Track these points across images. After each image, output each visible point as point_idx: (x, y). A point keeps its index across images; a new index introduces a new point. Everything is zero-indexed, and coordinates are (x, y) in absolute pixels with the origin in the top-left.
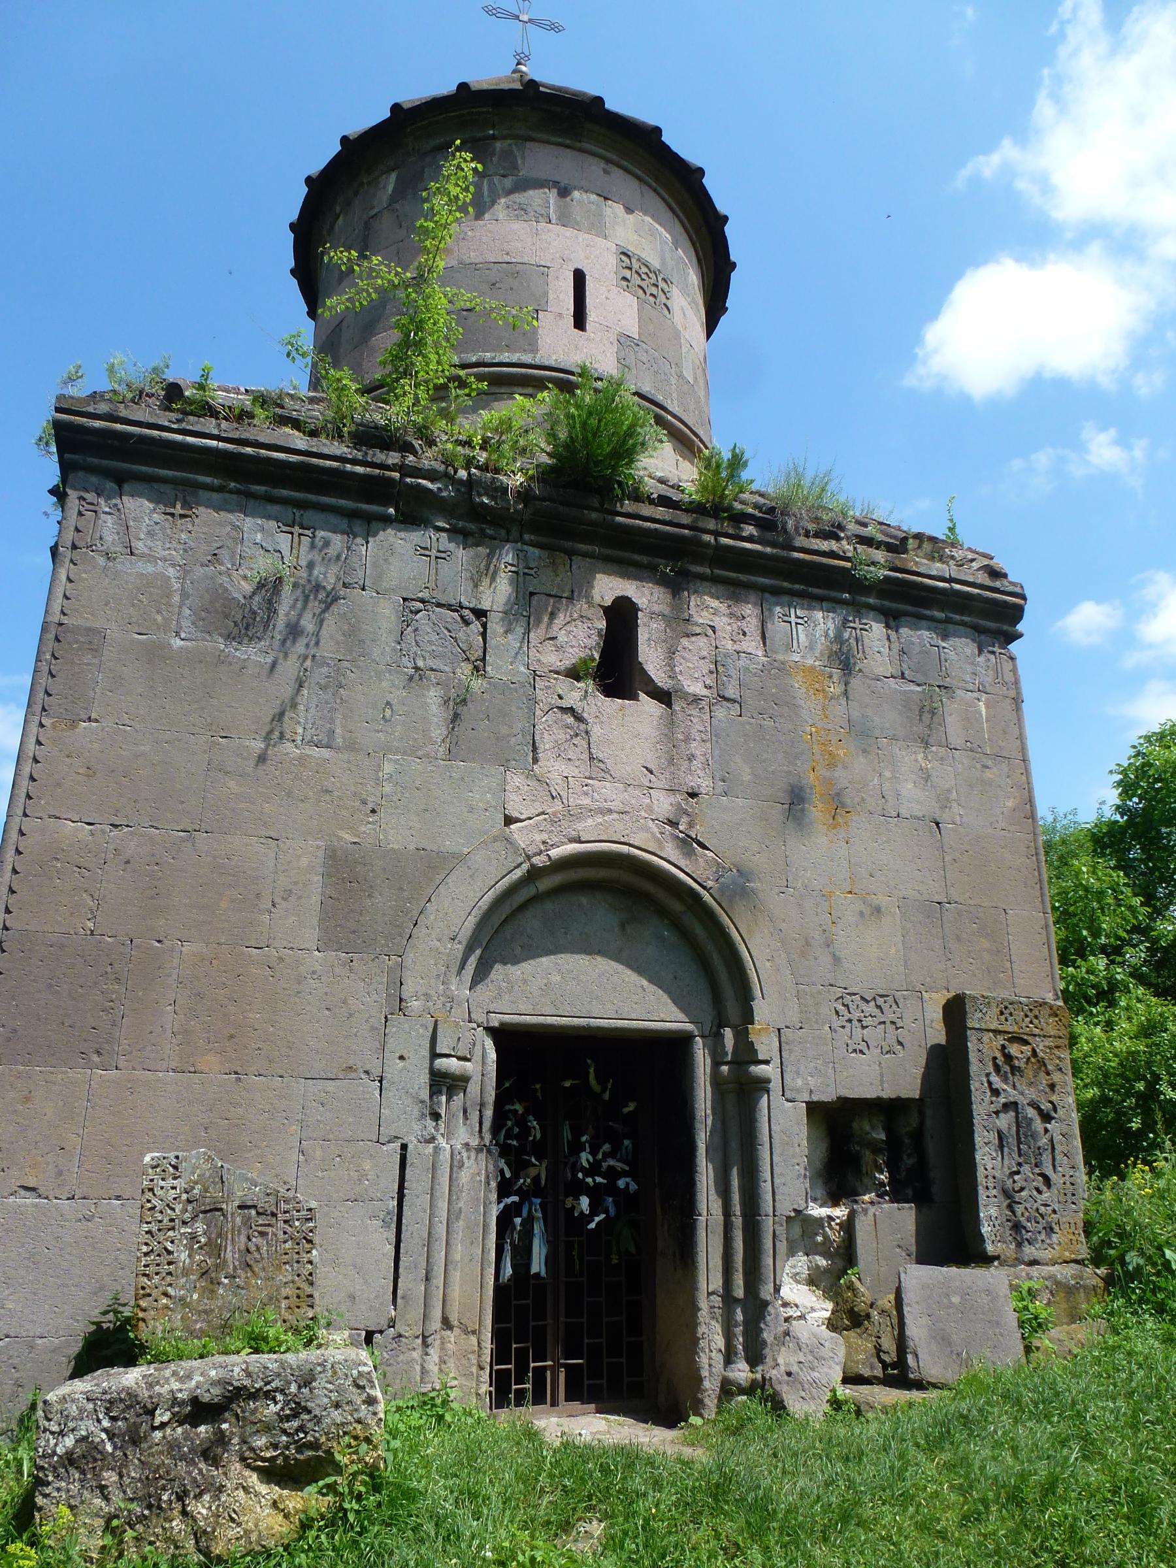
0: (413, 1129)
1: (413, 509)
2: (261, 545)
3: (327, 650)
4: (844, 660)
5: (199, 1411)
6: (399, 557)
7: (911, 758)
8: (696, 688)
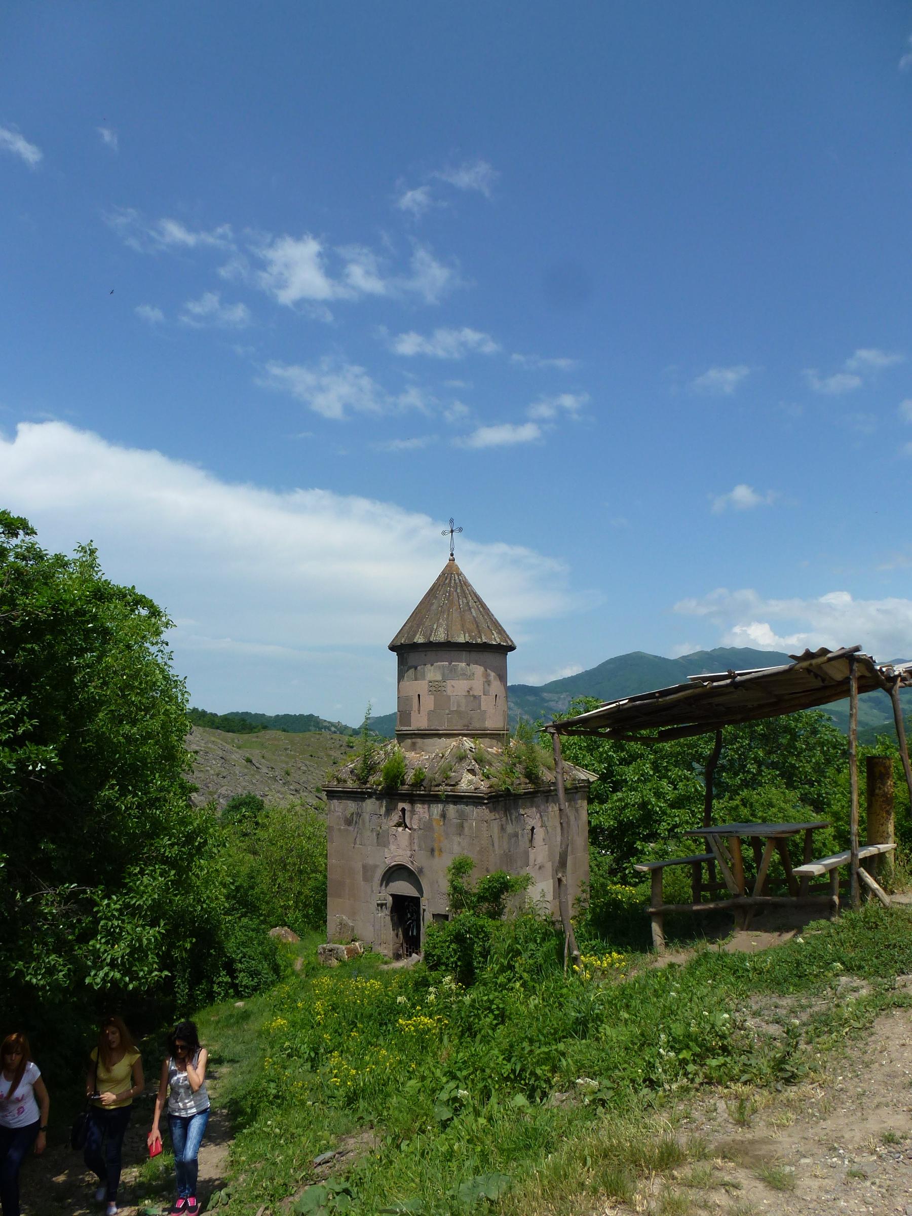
0: (375, 912)
1: (370, 795)
2: (351, 806)
3: (361, 826)
4: (444, 816)
5: (330, 951)
6: (370, 805)
7: (457, 839)
8: (415, 827)
